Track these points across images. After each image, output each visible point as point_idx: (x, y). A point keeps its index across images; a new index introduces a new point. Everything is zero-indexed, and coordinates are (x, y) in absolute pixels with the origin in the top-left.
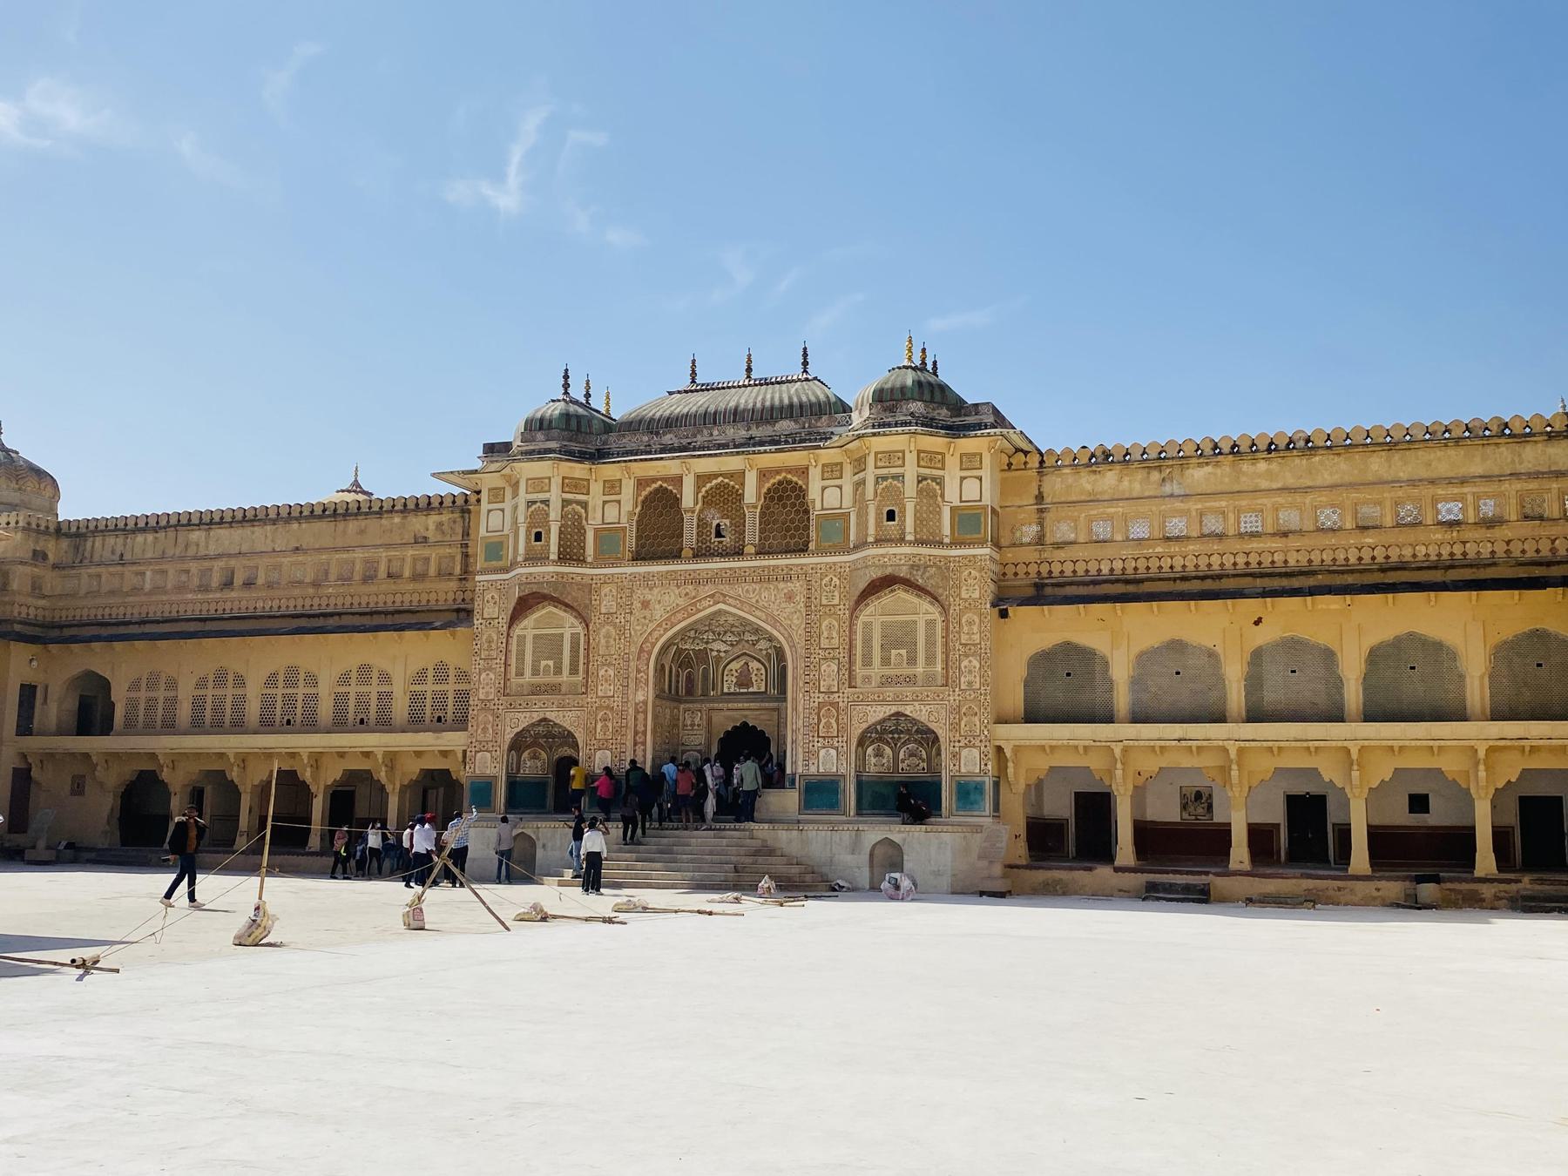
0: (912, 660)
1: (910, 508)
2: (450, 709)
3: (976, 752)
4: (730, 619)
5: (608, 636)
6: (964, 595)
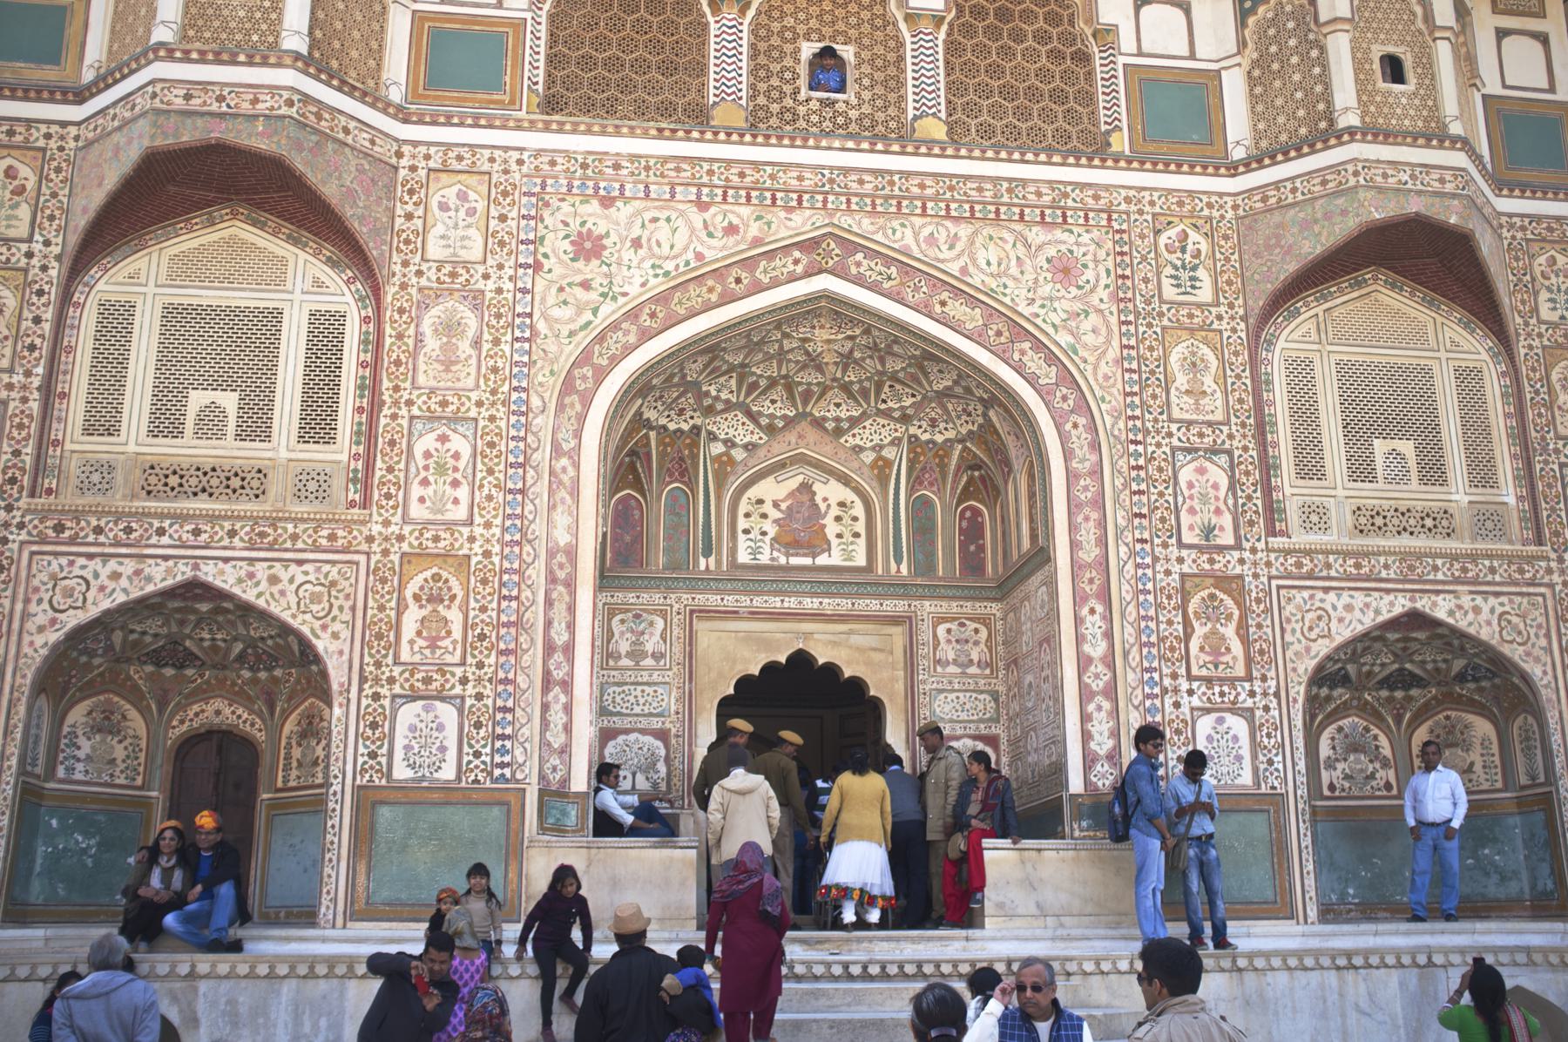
0: (1434, 472)
5: (450, 328)
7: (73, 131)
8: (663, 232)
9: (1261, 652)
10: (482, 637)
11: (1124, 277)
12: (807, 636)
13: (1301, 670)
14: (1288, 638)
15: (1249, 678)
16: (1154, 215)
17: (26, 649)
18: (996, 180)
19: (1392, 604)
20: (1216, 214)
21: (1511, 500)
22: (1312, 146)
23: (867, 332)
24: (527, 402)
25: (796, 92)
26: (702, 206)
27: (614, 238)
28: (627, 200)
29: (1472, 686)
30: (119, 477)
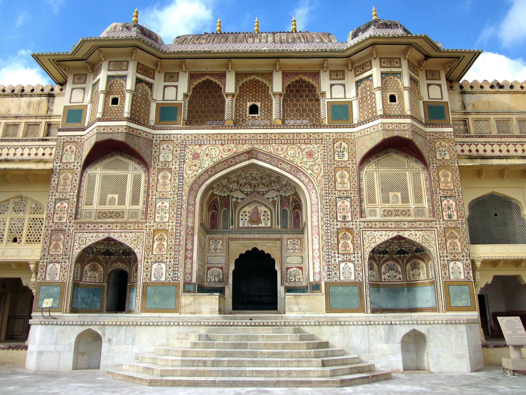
0: (405, 200)
1: (406, 94)
2: (25, 232)
3: (460, 264)
4: (255, 173)
5: (165, 177)
6: (438, 157)
7: (83, 137)
8: (213, 152)
9: (357, 247)
10: (171, 248)
11: (325, 155)
12: (256, 244)
13: (368, 251)
14: (365, 243)
15: (354, 254)
16: (333, 140)
17: (74, 253)
18: (293, 134)
19: (393, 234)
20: (349, 138)
21: (427, 206)
22: (371, 120)
23: (264, 171)
24: (182, 194)
25: (246, 115)
26: (222, 145)
27: (202, 154)
28: (205, 145)
29: (419, 253)
30: (93, 215)
